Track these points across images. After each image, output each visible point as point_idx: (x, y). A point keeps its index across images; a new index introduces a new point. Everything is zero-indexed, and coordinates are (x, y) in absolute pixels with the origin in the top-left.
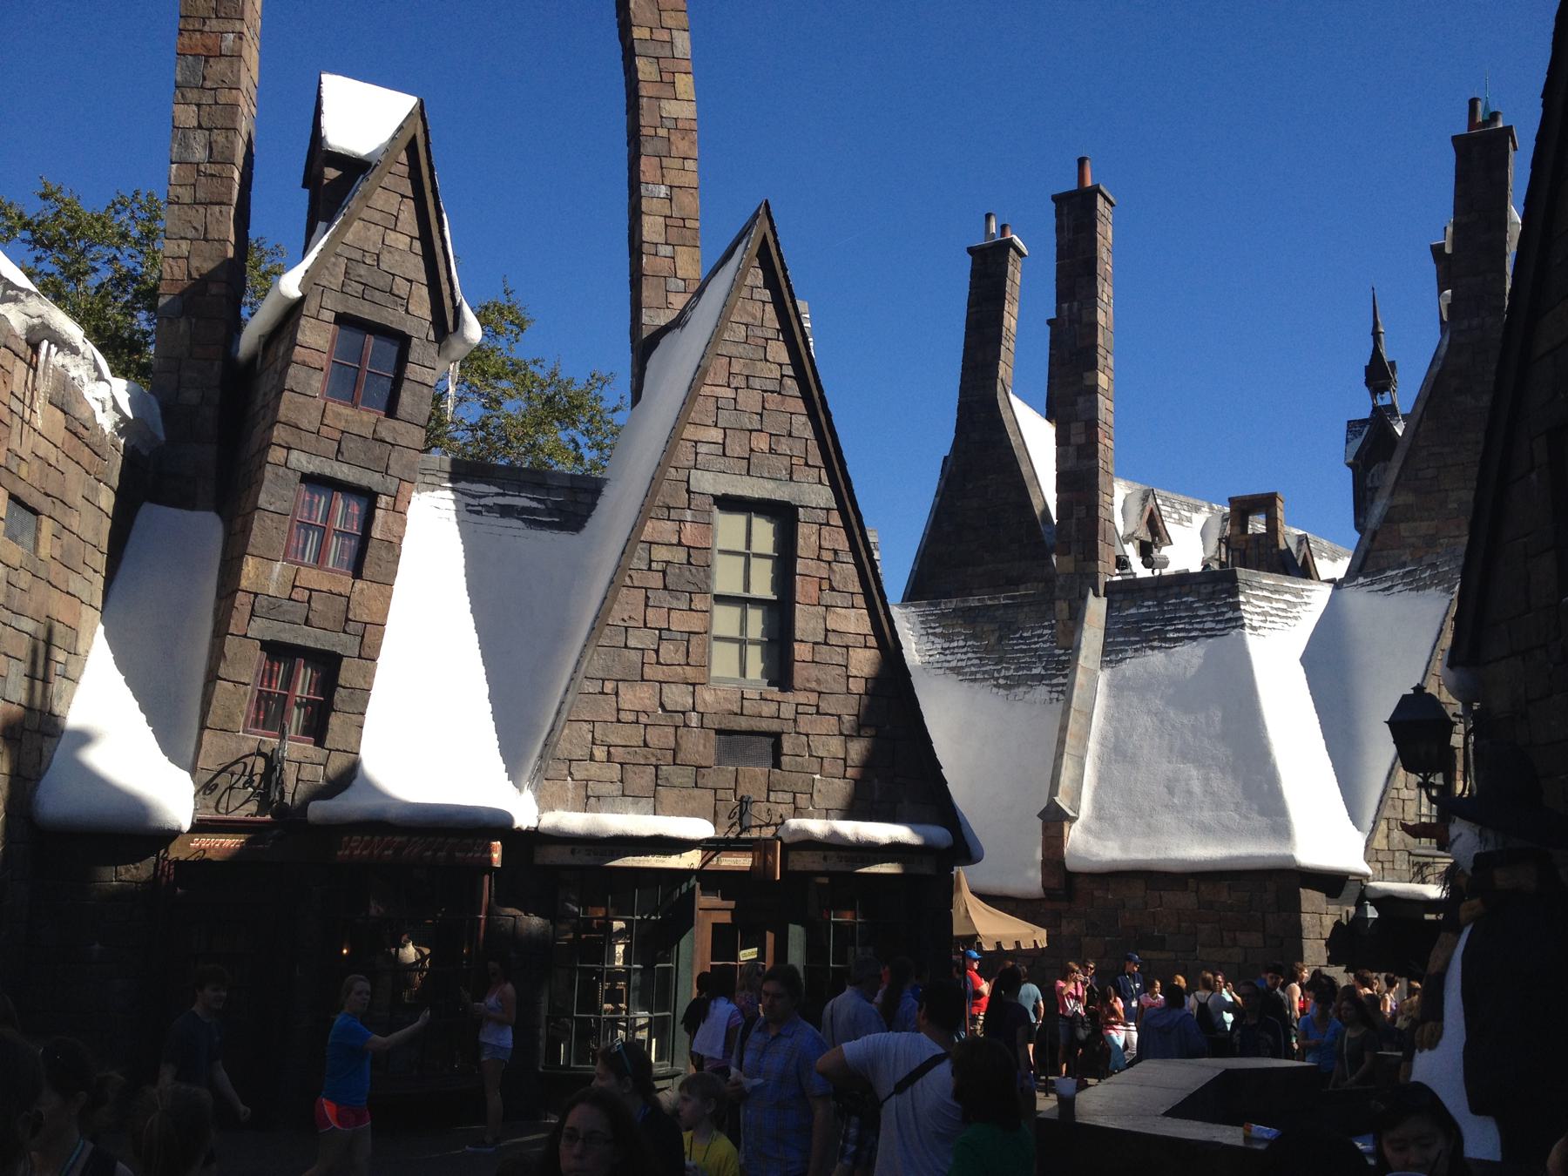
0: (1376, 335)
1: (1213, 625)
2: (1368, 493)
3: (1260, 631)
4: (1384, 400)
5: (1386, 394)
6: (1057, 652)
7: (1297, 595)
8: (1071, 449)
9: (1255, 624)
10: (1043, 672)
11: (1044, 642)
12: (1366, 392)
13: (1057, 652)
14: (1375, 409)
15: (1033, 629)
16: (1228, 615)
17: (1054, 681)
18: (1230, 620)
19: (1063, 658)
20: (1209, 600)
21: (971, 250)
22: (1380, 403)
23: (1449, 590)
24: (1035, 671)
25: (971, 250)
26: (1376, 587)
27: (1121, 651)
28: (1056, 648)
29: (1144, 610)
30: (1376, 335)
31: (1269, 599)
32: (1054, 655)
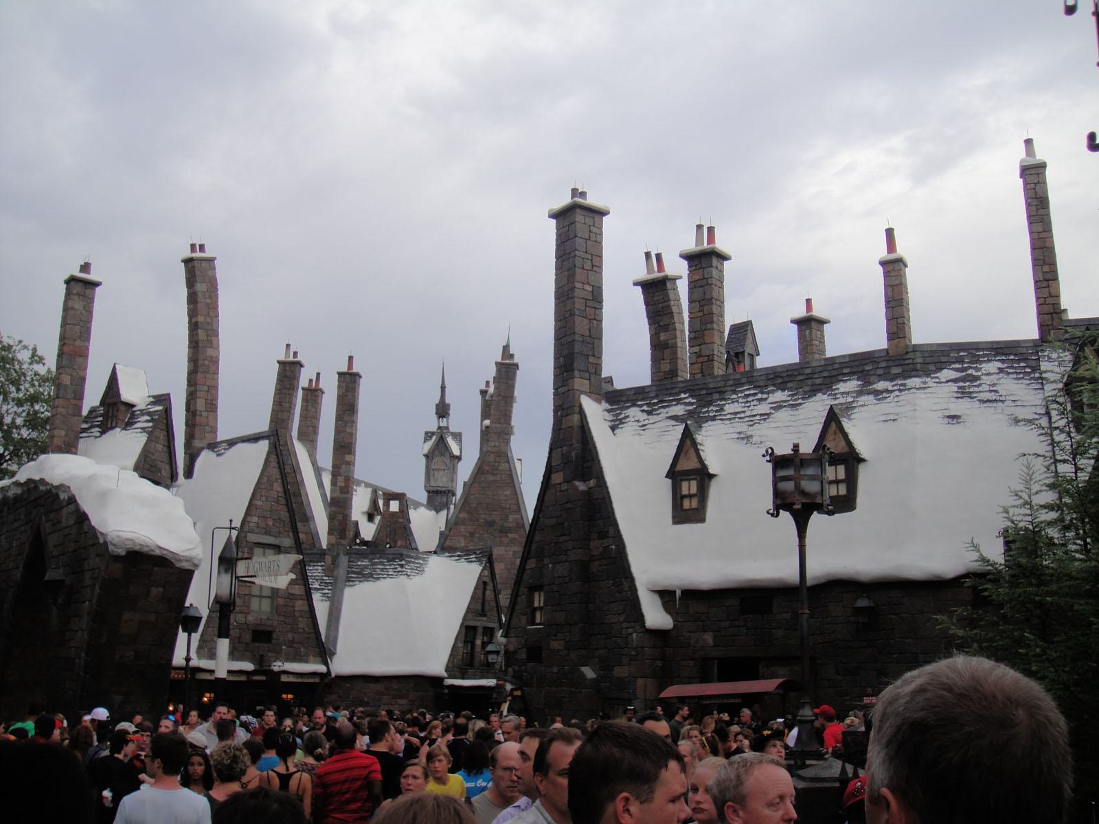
0: (443, 388)
1: (392, 573)
2: (432, 472)
3: (411, 577)
4: (443, 423)
5: (445, 419)
6: (325, 578)
7: (424, 561)
8: (338, 488)
9: (409, 574)
10: (319, 587)
11: (319, 573)
12: (435, 417)
13: (325, 578)
14: (439, 428)
15: (314, 566)
16: (399, 569)
17: (324, 592)
18: (399, 572)
19: (327, 581)
20: (392, 561)
21: (279, 362)
22: (441, 425)
23: (480, 564)
24: (314, 586)
25: (279, 362)
26: (453, 558)
27: (353, 581)
28: (325, 576)
29: (364, 563)
30: (443, 388)
31: (414, 563)
32: (323, 580)
